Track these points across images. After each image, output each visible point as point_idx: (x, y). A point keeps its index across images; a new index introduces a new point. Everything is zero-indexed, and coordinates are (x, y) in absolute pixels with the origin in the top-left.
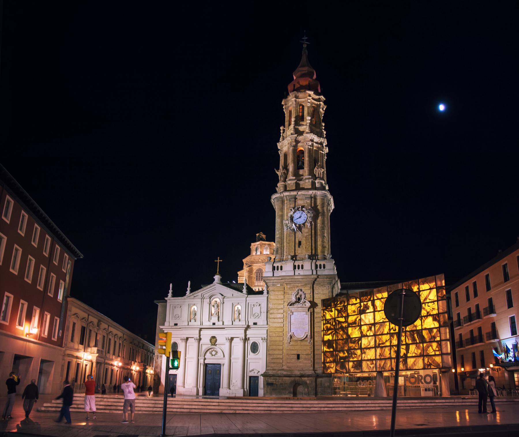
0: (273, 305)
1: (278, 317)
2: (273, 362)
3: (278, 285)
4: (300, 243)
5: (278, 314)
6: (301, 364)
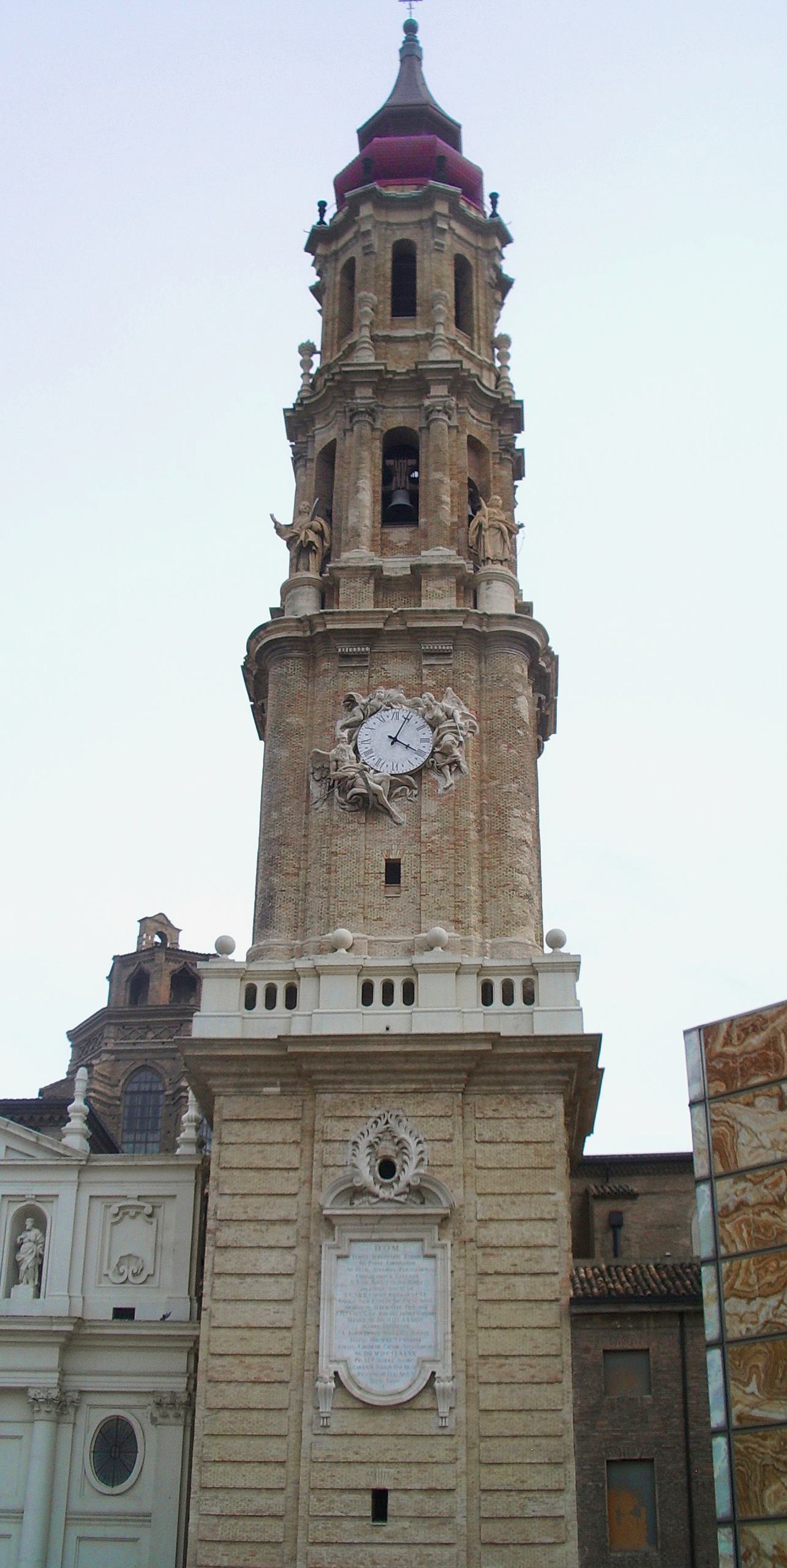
0: (237, 1198)
1: (265, 1268)
2: (224, 1538)
3: (266, 1090)
4: (393, 872)
5: (267, 1252)
6: (395, 1551)
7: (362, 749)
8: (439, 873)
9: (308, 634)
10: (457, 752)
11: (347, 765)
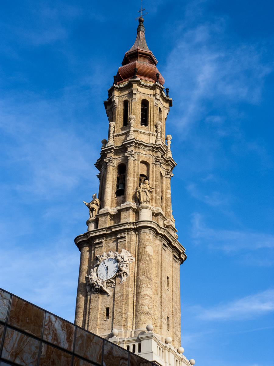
7: (98, 274)
8: (119, 310)
9: (87, 239)
10: (124, 269)
11: (93, 279)
